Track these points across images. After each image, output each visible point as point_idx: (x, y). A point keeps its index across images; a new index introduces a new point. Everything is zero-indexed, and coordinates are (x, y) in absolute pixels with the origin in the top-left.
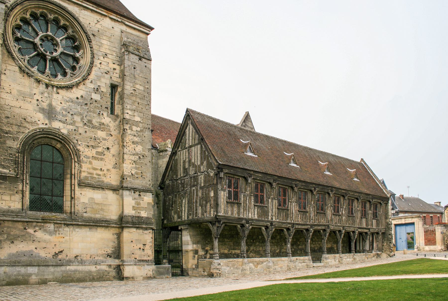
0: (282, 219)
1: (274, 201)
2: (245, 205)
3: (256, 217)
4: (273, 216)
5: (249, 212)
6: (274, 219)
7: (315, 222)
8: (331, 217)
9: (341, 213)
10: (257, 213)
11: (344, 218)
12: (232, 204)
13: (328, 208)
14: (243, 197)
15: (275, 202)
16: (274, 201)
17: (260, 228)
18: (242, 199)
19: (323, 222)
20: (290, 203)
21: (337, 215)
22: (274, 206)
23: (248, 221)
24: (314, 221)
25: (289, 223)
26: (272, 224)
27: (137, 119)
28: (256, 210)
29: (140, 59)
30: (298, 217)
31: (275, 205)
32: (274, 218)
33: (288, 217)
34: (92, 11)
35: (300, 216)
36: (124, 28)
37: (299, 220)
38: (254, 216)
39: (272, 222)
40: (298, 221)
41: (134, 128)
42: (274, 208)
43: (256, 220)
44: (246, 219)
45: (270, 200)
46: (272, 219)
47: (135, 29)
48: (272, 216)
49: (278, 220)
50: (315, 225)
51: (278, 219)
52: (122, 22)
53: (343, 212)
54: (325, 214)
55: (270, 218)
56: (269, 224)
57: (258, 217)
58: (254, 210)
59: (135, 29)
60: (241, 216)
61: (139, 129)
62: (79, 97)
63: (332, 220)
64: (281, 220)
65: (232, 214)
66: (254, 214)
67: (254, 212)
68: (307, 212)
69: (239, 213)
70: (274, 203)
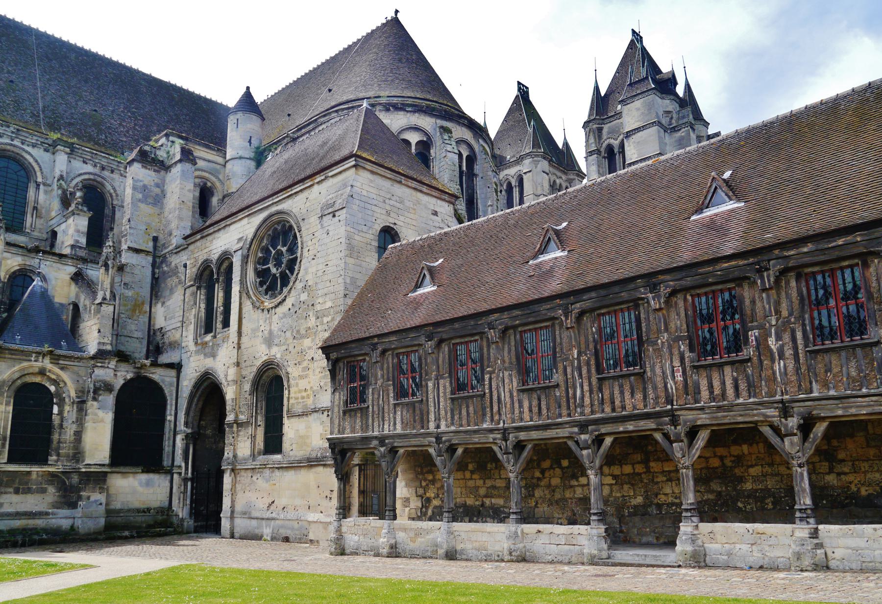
0: (464, 422)
1: (441, 382)
2: (376, 408)
3: (399, 430)
4: (439, 420)
5: (383, 421)
6: (443, 428)
7: (593, 412)
8: (685, 380)
9: (749, 351)
10: (402, 419)
11: (779, 366)
12: (353, 413)
13: (658, 351)
14: (373, 393)
15: (445, 384)
16: (441, 382)
17: (427, 451)
18: (371, 398)
19: (633, 402)
20: (487, 377)
21: (720, 366)
22: (441, 394)
23: (382, 440)
24: (588, 410)
25: (491, 431)
26: (438, 438)
27: (329, 304)
28: (399, 413)
29: (334, 216)
30: (521, 406)
31: (445, 393)
32: (443, 424)
33: (484, 415)
34: (301, 191)
35: (526, 404)
36: (331, 182)
37: (526, 416)
38: (395, 429)
39: (438, 434)
40: (521, 420)
41: (325, 320)
42: (441, 399)
43: (400, 436)
44: (376, 438)
45: (430, 384)
46: (438, 427)
47: (340, 173)
48: (438, 419)
49: (453, 428)
50: (596, 422)
51: (452, 424)
52: (326, 178)
53: (772, 342)
54: (641, 375)
55: (432, 425)
56: (434, 440)
57: (403, 429)
58: (395, 412)
59: (340, 173)
60: (370, 433)
61: (329, 319)
62: (290, 306)
63: (690, 390)
64: (461, 426)
65: (353, 431)
66: (395, 424)
67: (395, 418)
68: (557, 386)
69: (365, 428)
70: (441, 389)
